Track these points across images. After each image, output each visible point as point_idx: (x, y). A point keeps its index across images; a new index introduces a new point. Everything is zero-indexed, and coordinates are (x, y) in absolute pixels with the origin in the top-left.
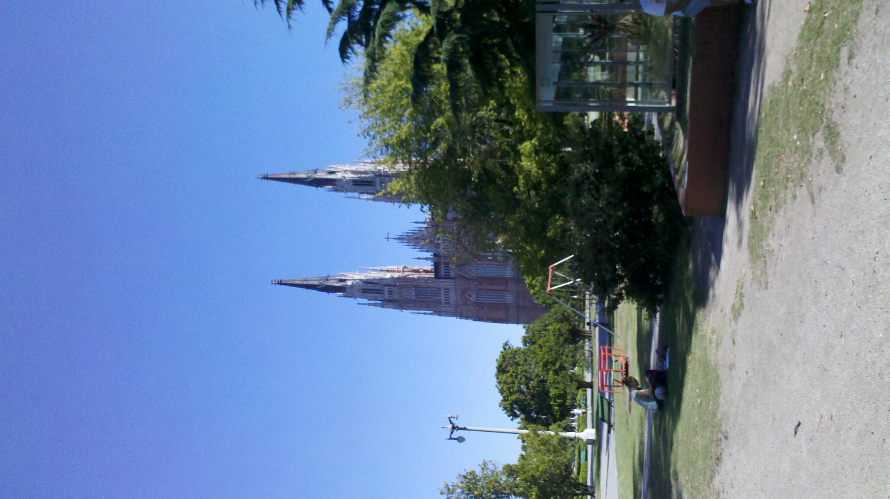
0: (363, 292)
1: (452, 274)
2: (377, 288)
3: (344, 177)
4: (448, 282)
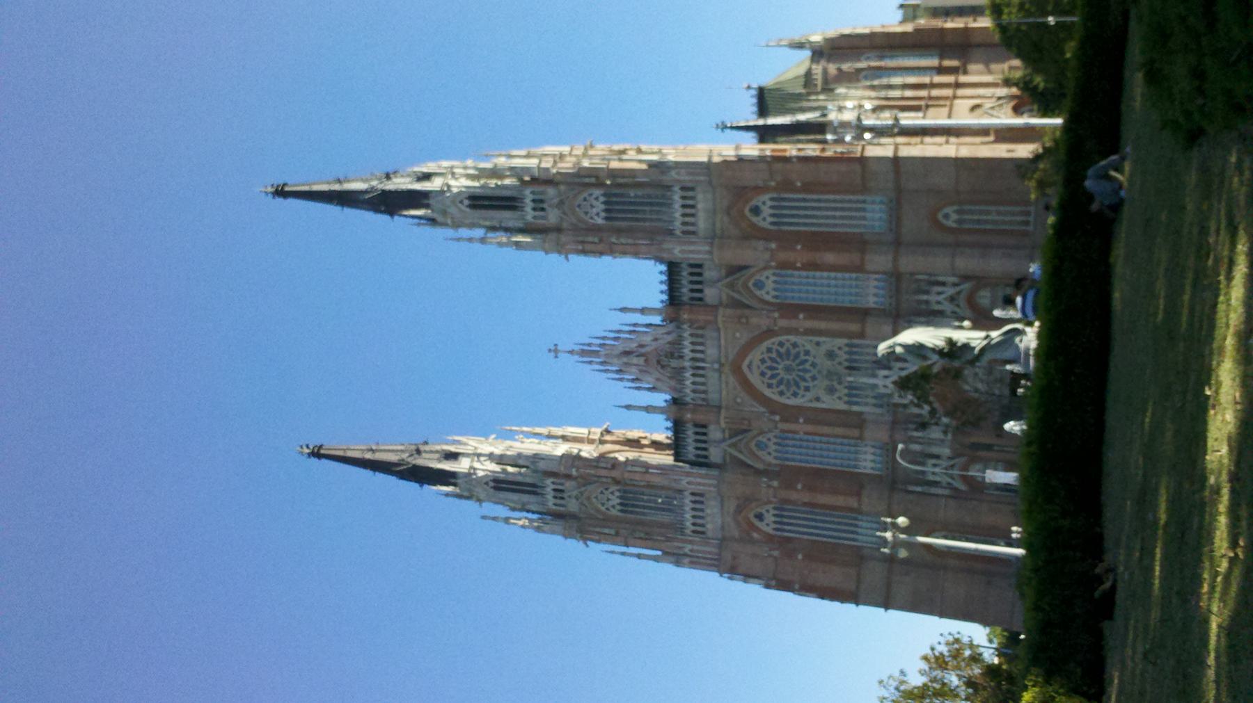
0: (495, 488)
1: (715, 454)
3: (449, 186)
4: (701, 476)
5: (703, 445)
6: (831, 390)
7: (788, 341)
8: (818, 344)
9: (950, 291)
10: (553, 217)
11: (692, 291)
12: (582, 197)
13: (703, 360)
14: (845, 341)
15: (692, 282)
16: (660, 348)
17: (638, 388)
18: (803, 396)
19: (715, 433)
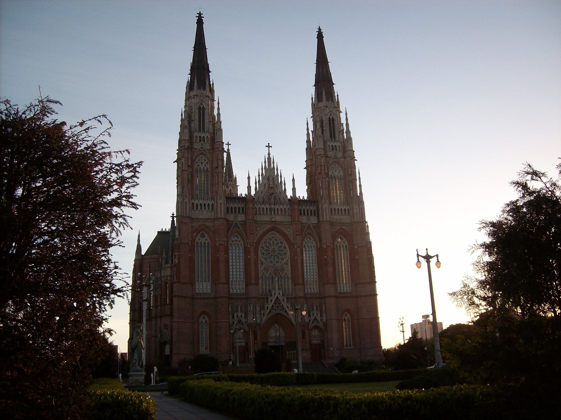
0: (199, 108)
2: (206, 125)
5: (234, 211)
6: (267, 270)
7: (287, 251)
8: (287, 264)
9: (319, 318)
10: (330, 154)
11: (304, 210)
12: (339, 167)
13: (274, 213)
14: (290, 277)
15: (308, 211)
16: (276, 194)
17: (256, 183)
18: (263, 257)
19: (241, 217)
